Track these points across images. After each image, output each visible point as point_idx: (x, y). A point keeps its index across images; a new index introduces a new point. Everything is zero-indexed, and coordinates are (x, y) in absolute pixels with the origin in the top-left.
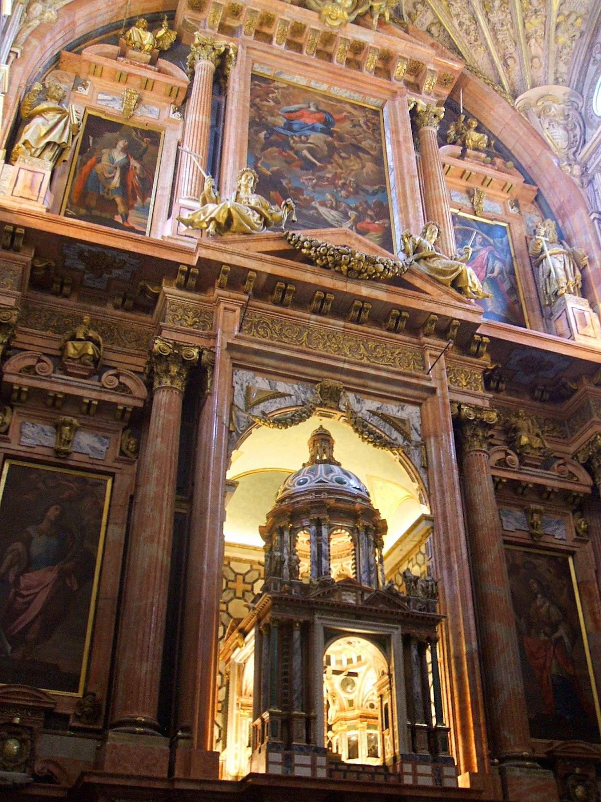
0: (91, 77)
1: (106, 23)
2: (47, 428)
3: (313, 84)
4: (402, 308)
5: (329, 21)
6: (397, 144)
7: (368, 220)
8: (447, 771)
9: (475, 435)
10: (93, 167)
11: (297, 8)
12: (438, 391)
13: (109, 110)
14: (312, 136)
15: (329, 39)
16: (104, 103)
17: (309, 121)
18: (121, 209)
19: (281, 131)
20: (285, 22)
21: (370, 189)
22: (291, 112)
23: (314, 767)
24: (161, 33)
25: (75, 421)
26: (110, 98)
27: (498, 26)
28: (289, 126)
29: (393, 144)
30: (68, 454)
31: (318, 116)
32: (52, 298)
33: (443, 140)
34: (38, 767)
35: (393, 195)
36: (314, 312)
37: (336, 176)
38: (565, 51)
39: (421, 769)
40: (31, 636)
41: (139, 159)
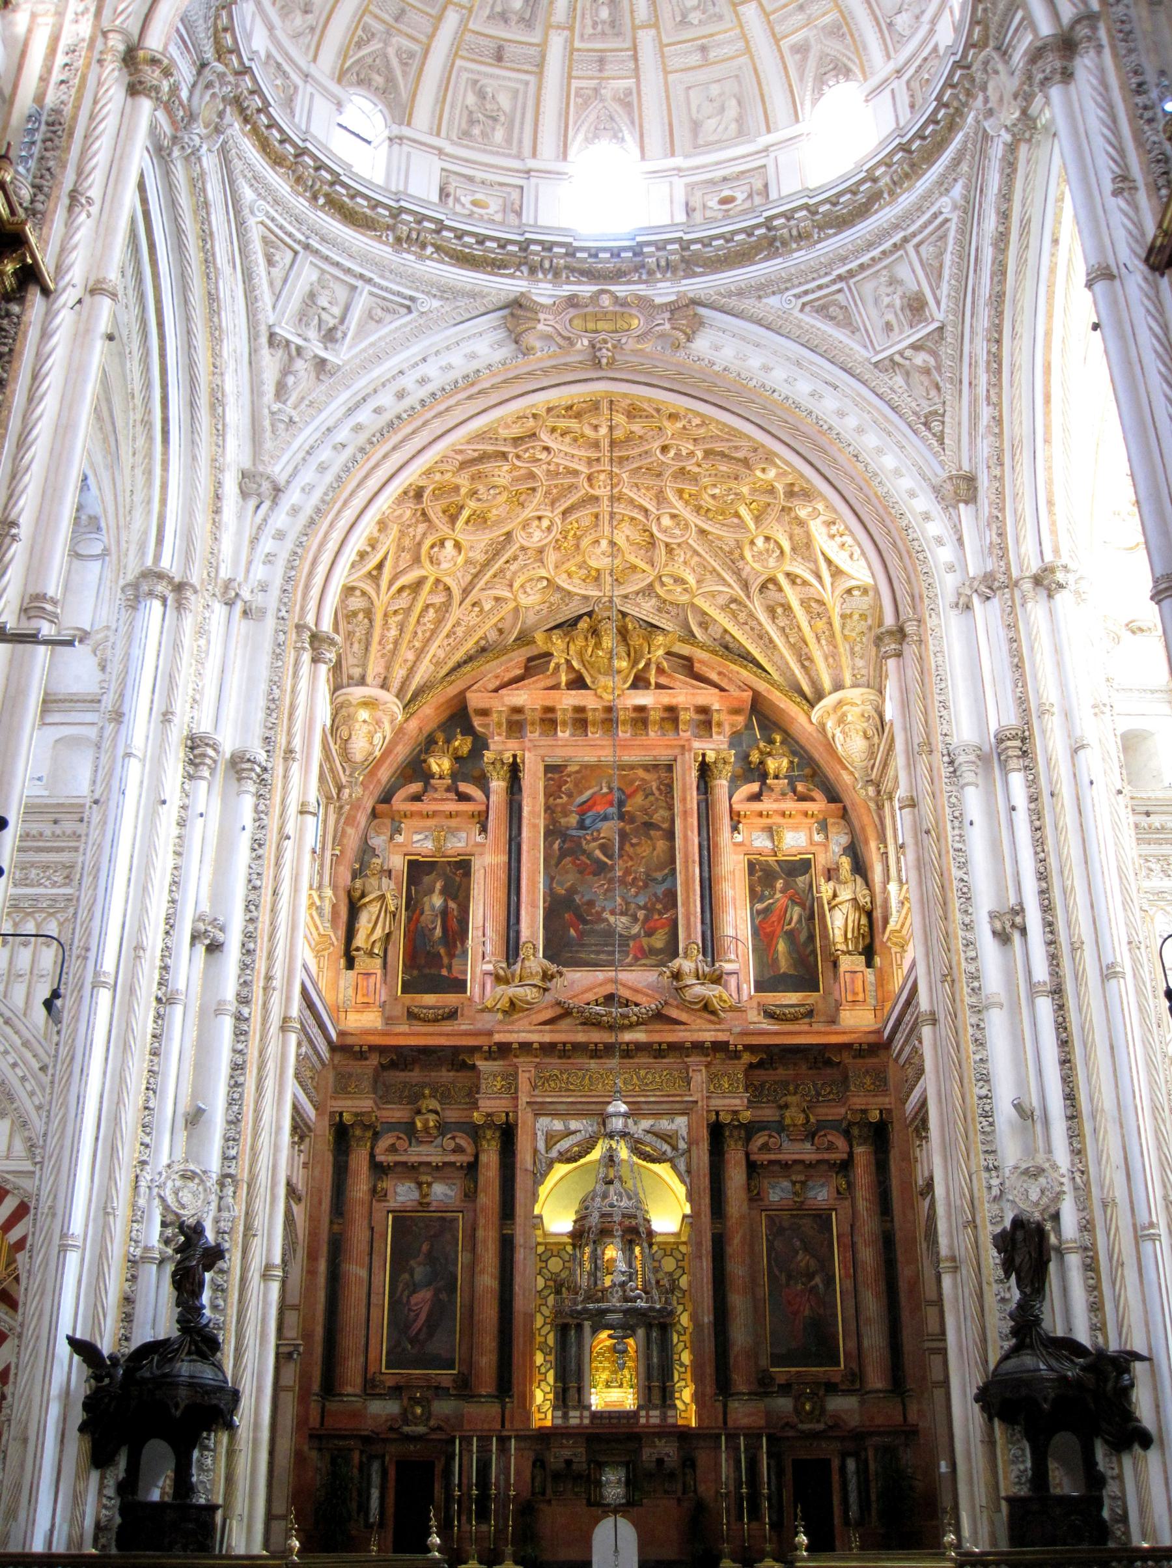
2: (413, 1185)
4: (660, 1044)
7: (656, 917)
8: (670, 1413)
9: (731, 1136)
10: (418, 921)
13: (425, 852)
15: (609, 709)
17: (600, 809)
18: (446, 961)
19: (574, 833)
21: (659, 876)
23: (581, 1417)
25: (430, 1179)
28: (582, 826)
30: (428, 1204)
31: (609, 797)
32: (402, 1074)
34: (432, 1423)
36: (591, 1057)
37: (627, 872)
38: (857, 649)
39: (652, 1413)
40: (422, 1337)
41: (454, 899)
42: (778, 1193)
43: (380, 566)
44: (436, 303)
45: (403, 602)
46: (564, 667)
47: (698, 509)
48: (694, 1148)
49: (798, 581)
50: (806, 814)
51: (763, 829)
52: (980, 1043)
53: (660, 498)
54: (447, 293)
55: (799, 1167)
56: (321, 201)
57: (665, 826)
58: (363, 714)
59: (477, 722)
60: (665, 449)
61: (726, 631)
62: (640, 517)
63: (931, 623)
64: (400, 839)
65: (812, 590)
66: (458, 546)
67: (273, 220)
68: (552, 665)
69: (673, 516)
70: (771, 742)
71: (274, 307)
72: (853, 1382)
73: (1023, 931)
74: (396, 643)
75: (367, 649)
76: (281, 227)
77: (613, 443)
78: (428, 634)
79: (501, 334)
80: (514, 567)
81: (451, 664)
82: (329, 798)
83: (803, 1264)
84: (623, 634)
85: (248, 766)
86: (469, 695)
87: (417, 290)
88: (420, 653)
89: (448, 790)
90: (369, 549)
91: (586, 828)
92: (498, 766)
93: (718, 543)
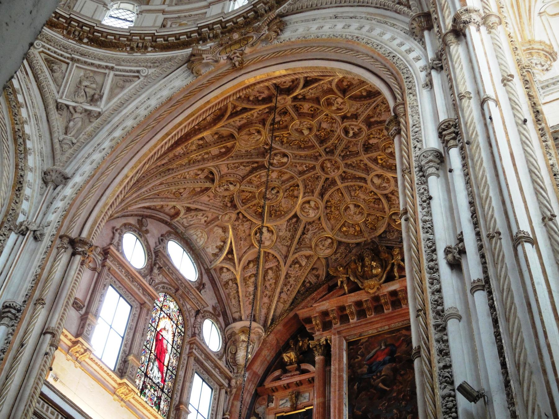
0: (274, 394)
1: (274, 355)
3: (380, 329)
5: (371, 291)
11: (353, 294)
13: (286, 409)
14: (384, 369)
15: (376, 299)
16: (282, 406)
17: (381, 359)
19: (366, 376)
20: (350, 306)
22: (371, 357)
24: (301, 344)
26: (284, 401)
28: (370, 371)
31: (386, 351)
37: (399, 392)
43: (231, 252)
44: (151, 71)
45: (252, 269)
46: (345, 282)
52: (444, 353)
54: (155, 63)
56: (85, 40)
58: (243, 337)
59: (308, 327)
60: (346, 132)
62: (361, 184)
63: (409, 99)
64: (272, 405)
66: (269, 231)
67: (49, 49)
68: (339, 283)
69: (379, 176)
71: (58, 92)
74: (255, 295)
75: (239, 301)
76: (55, 52)
77: (322, 141)
78: (273, 286)
79: (186, 74)
80: (309, 235)
81: (291, 301)
82: (221, 386)
84: (376, 255)
85: (7, 310)
86: (297, 312)
87: (140, 66)
88: (271, 298)
89: (297, 370)
90: (222, 244)
91: (374, 372)
92: (318, 348)
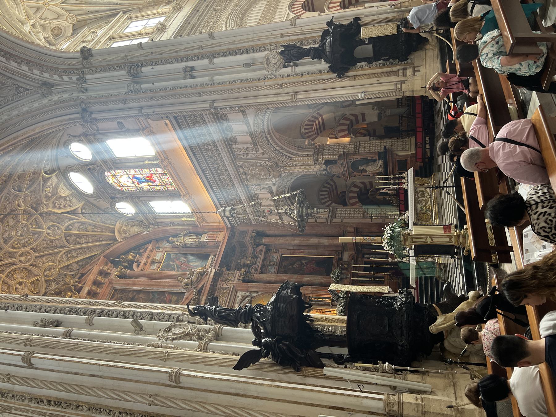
4: (209, 293)
6: (134, 285)
7: (165, 299)
12: (235, 285)
21: (151, 296)
27: (87, 241)
29: (134, 286)
33: (130, 267)
35: (155, 289)
38: (103, 220)
42: (273, 269)
47: (24, 246)
48: (250, 289)
49: (70, 227)
50: (151, 251)
51: (151, 266)
53: (11, 255)
55: (265, 262)
57: (135, 293)
61: (77, 262)
62: (15, 267)
65: (76, 225)
69: (22, 255)
70: (123, 258)
72: (339, 253)
73: (192, 69)
83: (297, 266)
93: (42, 247)
